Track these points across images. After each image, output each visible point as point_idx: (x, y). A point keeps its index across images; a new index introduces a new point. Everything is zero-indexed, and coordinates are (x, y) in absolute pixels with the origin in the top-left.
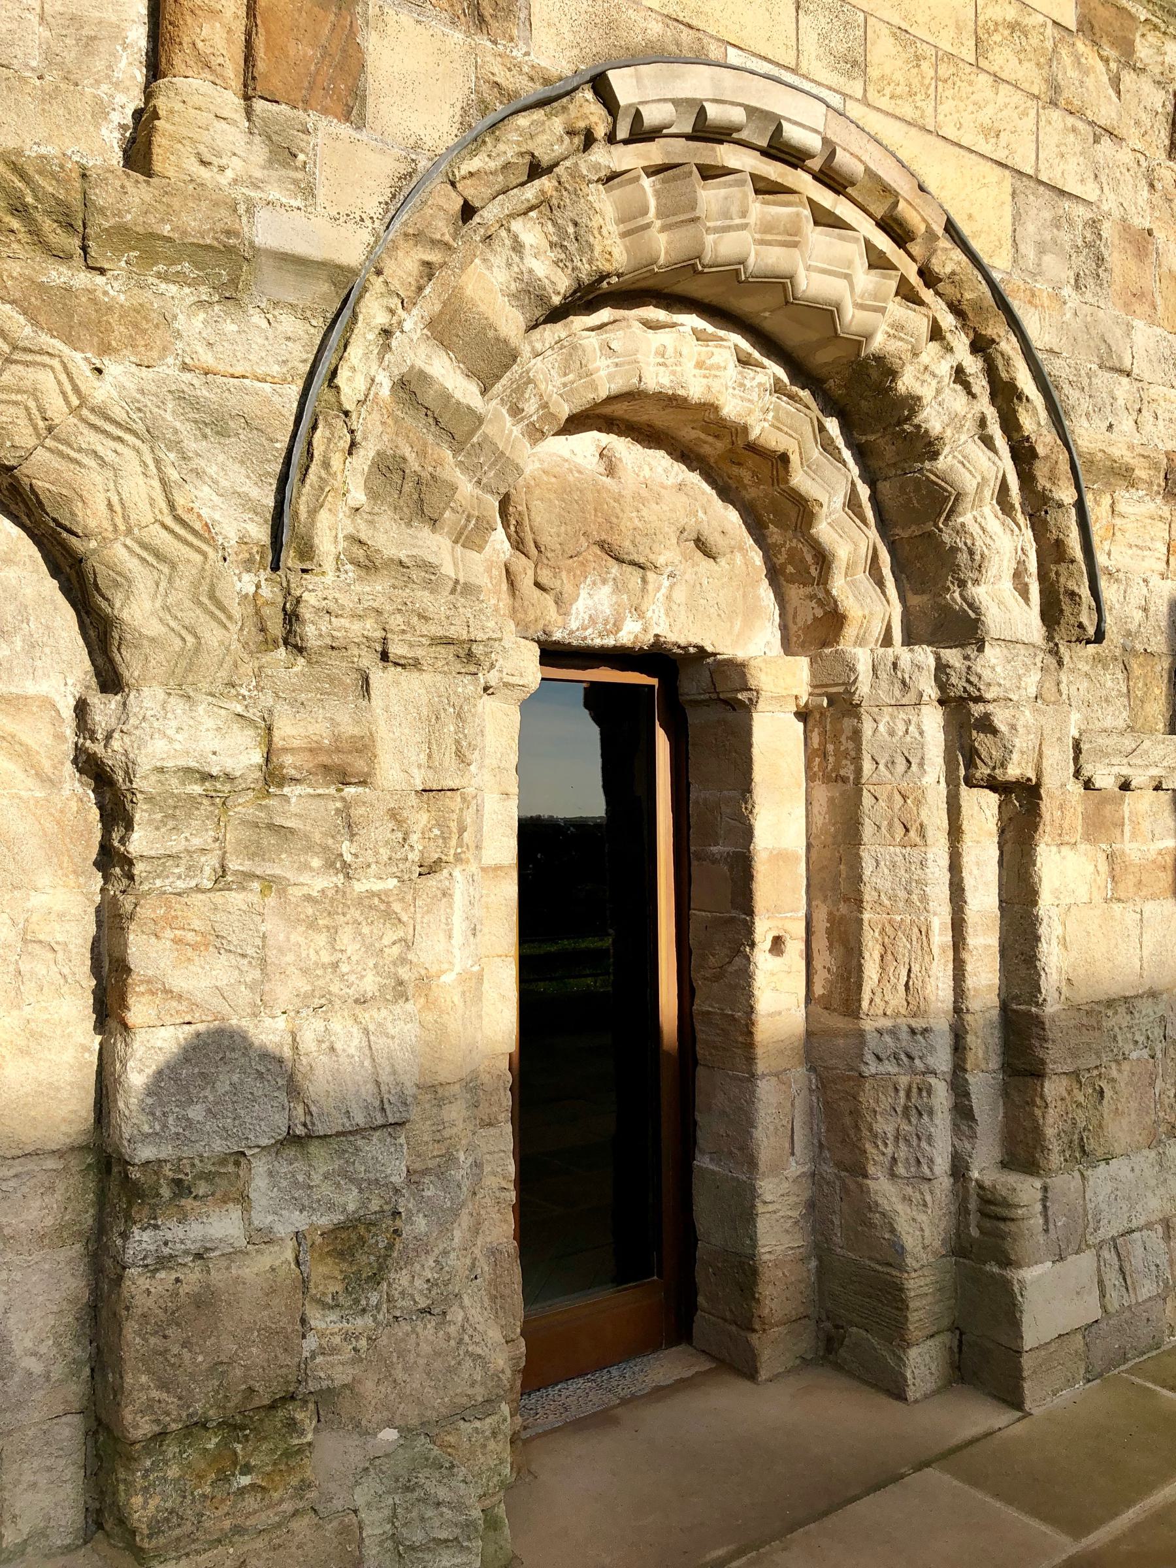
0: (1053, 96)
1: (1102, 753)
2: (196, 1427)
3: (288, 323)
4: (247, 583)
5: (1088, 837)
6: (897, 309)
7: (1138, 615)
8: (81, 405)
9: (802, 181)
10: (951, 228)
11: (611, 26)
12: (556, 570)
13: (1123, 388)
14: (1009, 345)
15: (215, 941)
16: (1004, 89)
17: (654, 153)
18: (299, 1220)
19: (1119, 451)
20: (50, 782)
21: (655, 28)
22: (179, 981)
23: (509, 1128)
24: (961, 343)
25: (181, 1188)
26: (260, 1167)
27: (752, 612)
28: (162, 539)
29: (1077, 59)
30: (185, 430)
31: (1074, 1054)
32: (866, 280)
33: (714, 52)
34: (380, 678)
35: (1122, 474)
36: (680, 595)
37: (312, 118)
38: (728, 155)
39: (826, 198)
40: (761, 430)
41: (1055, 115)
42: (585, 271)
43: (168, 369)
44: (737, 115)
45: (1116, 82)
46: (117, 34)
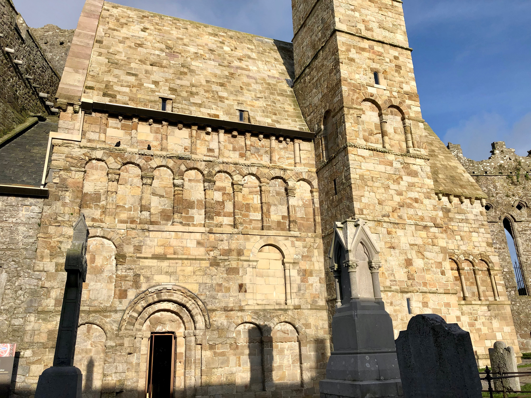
0: (206, 274)
1: (211, 340)
2: (107, 393)
3: (121, 314)
4: (116, 332)
5: (209, 350)
6: (185, 298)
7: (220, 325)
8: (106, 322)
9: (172, 291)
10: (189, 291)
11: (150, 285)
12: (154, 325)
13: (217, 301)
14: (198, 300)
15: (111, 358)
16: (197, 276)
17: (155, 293)
18: (116, 379)
19: (214, 308)
20: (102, 347)
21: (154, 284)
22: (108, 360)
23: (144, 379)
24: (193, 300)
25: (107, 375)
26: (113, 374)
27: (180, 327)
28: (110, 330)
29: (210, 270)
30: (112, 322)
31: (206, 373)
32: (181, 296)
33: (160, 284)
34: (125, 338)
35: (214, 310)
36: (170, 326)
37: (123, 300)
38: (162, 291)
39: (174, 291)
40: (175, 310)
41: (205, 276)
42: (148, 303)
43: (112, 319)
44: (162, 289)
45: (217, 269)
46: (112, 296)
